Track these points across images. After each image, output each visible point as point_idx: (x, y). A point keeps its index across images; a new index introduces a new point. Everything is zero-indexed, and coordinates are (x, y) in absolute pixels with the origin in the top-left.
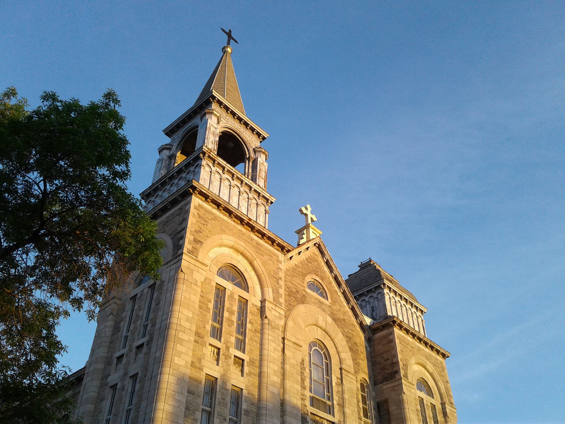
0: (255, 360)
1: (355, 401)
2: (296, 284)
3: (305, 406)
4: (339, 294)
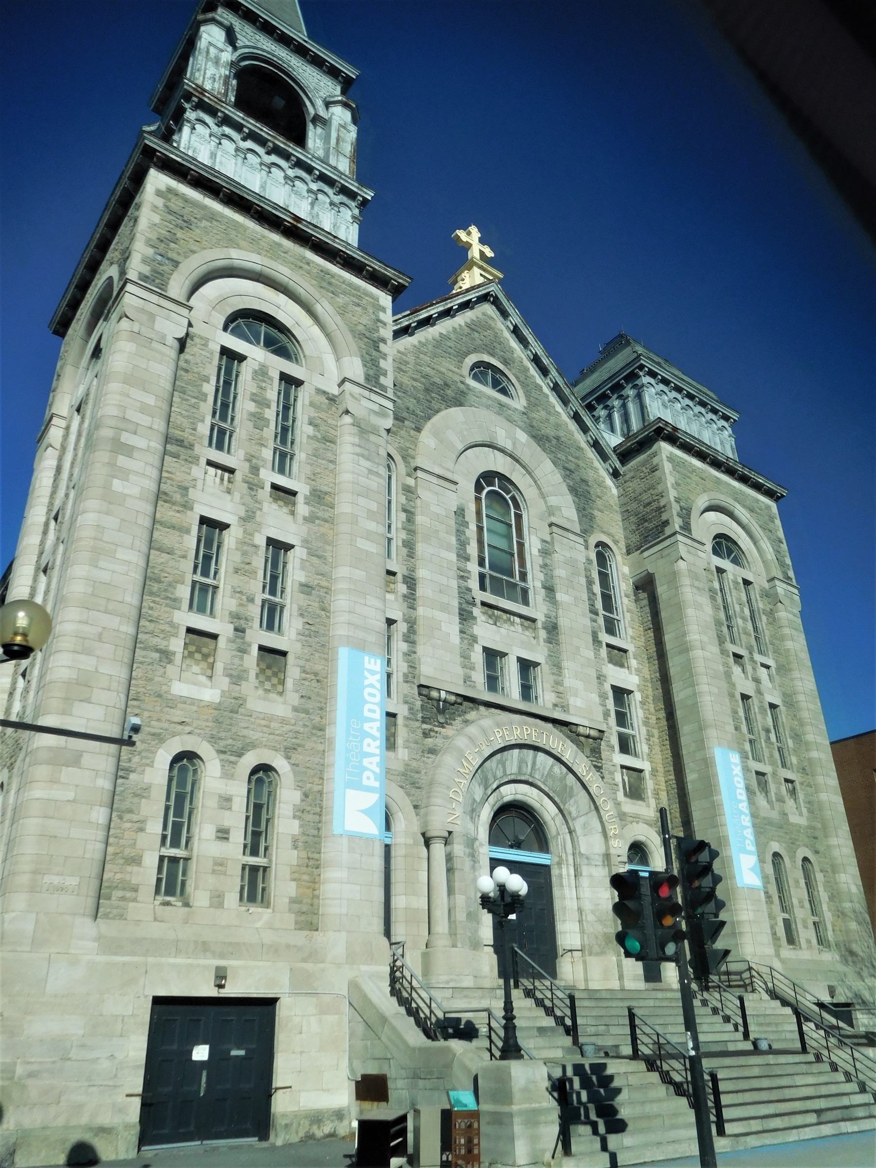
0: (326, 493)
1: (583, 581)
2: (443, 370)
3: (469, 590)
4: (546, 390)
